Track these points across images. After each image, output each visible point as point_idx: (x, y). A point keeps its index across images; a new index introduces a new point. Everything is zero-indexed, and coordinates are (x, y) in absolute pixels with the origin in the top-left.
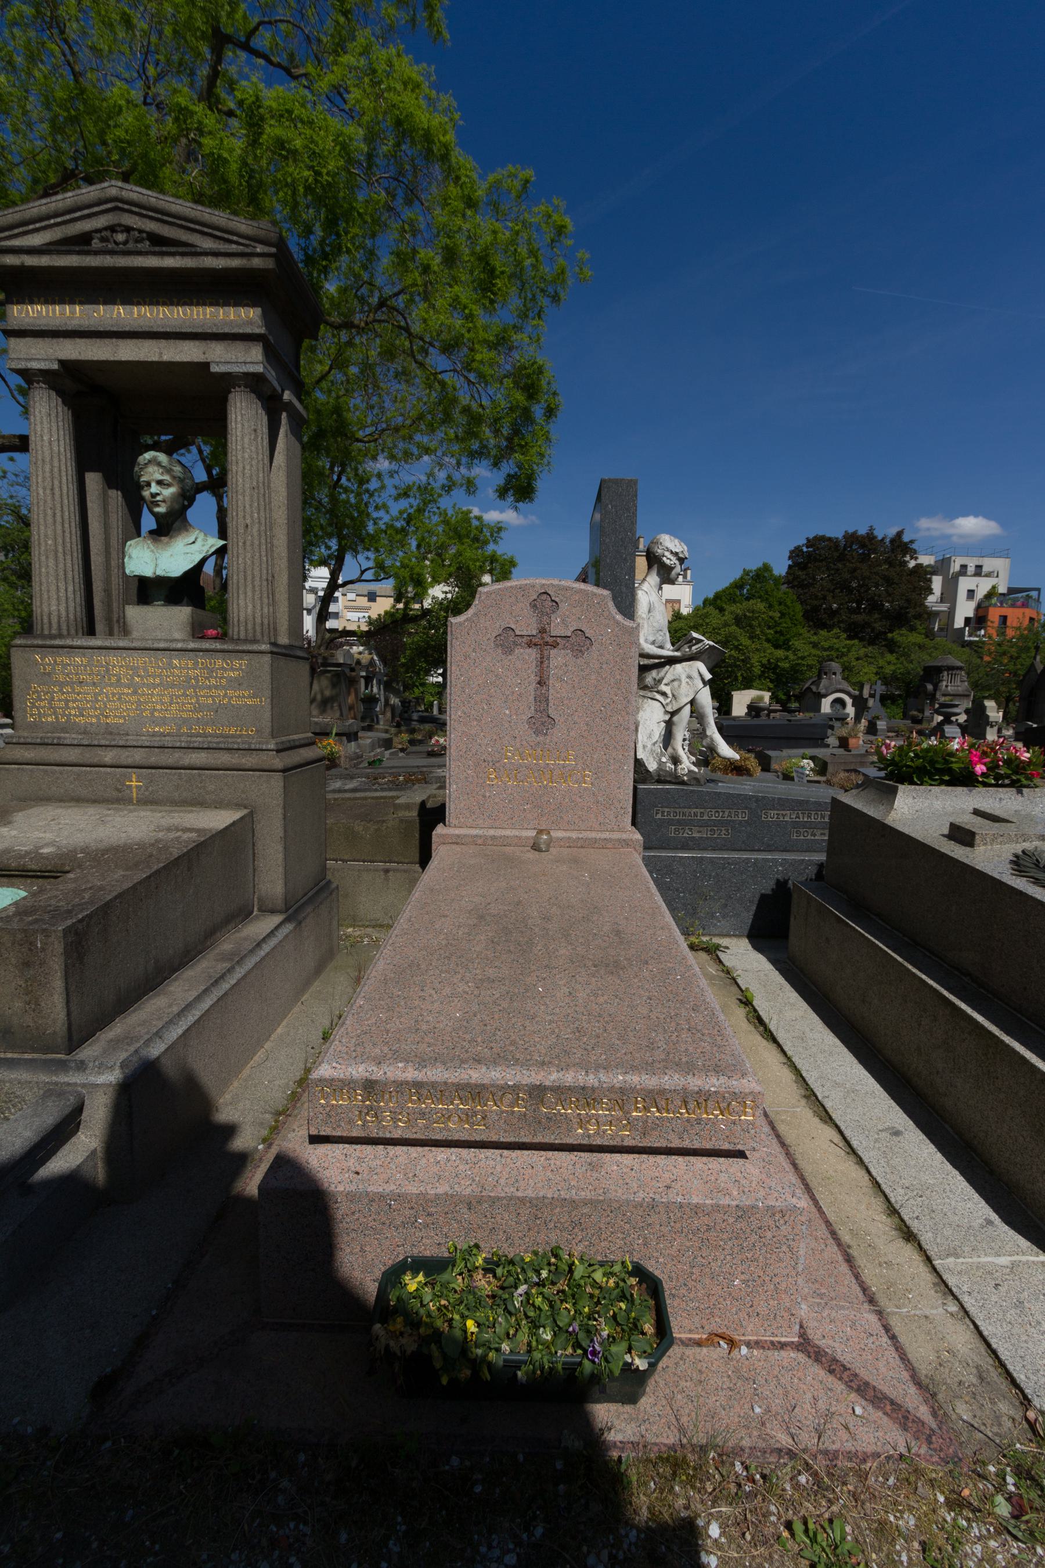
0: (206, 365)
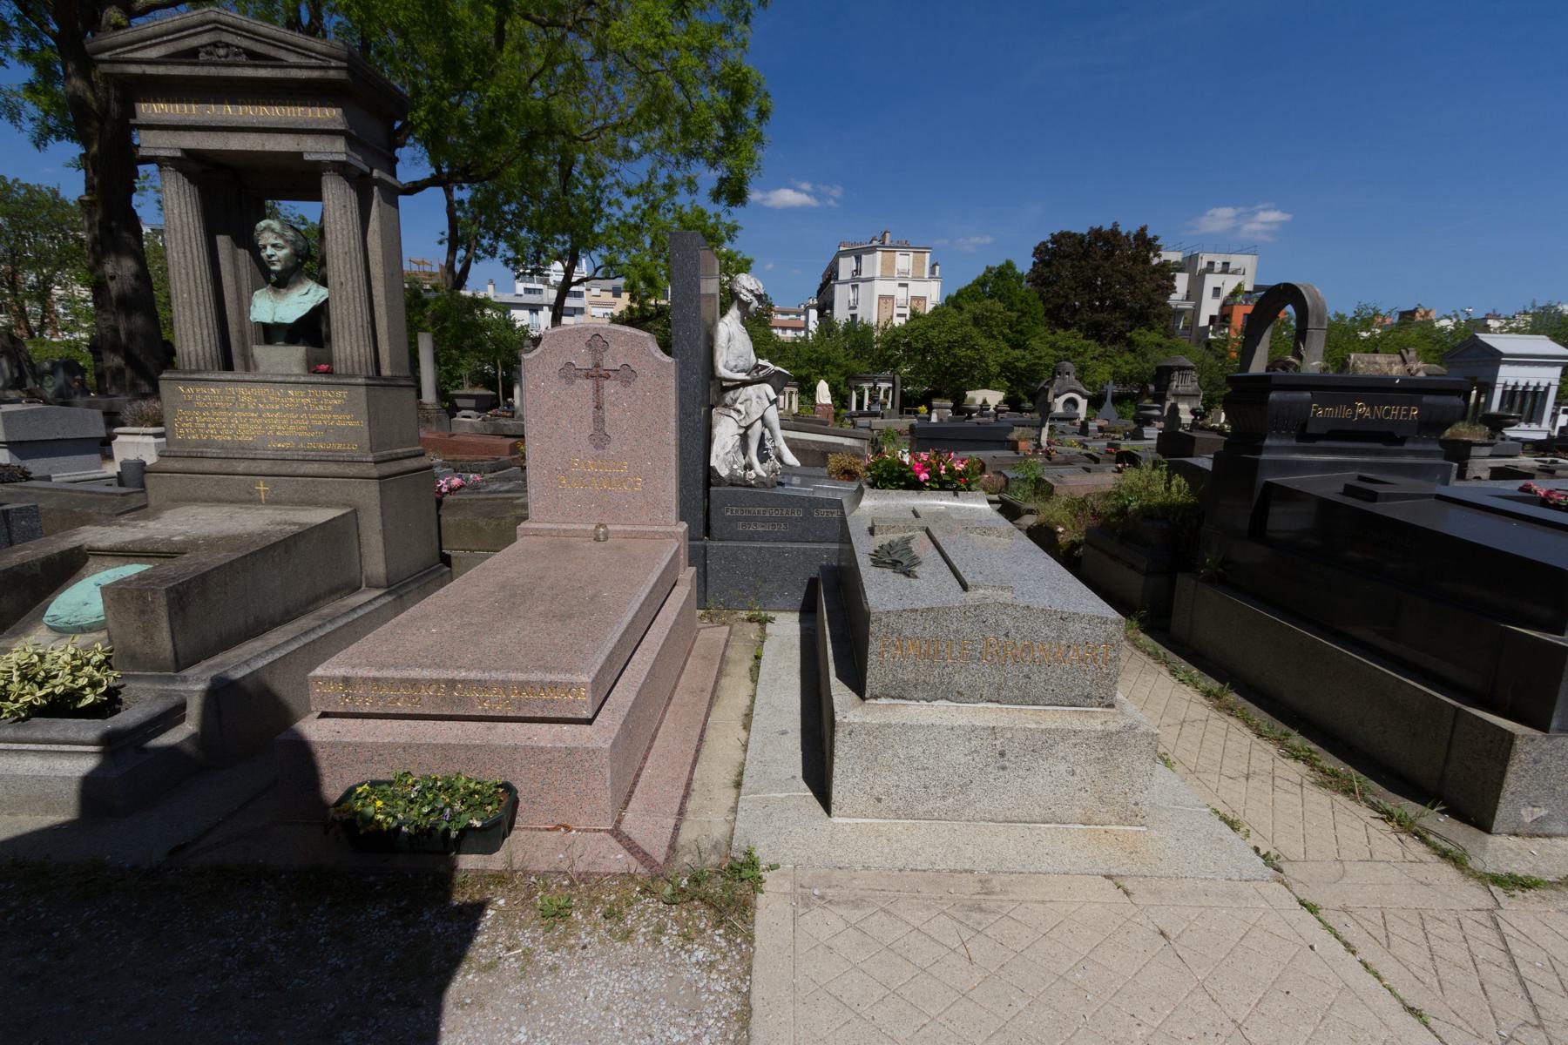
0: (301, 154)
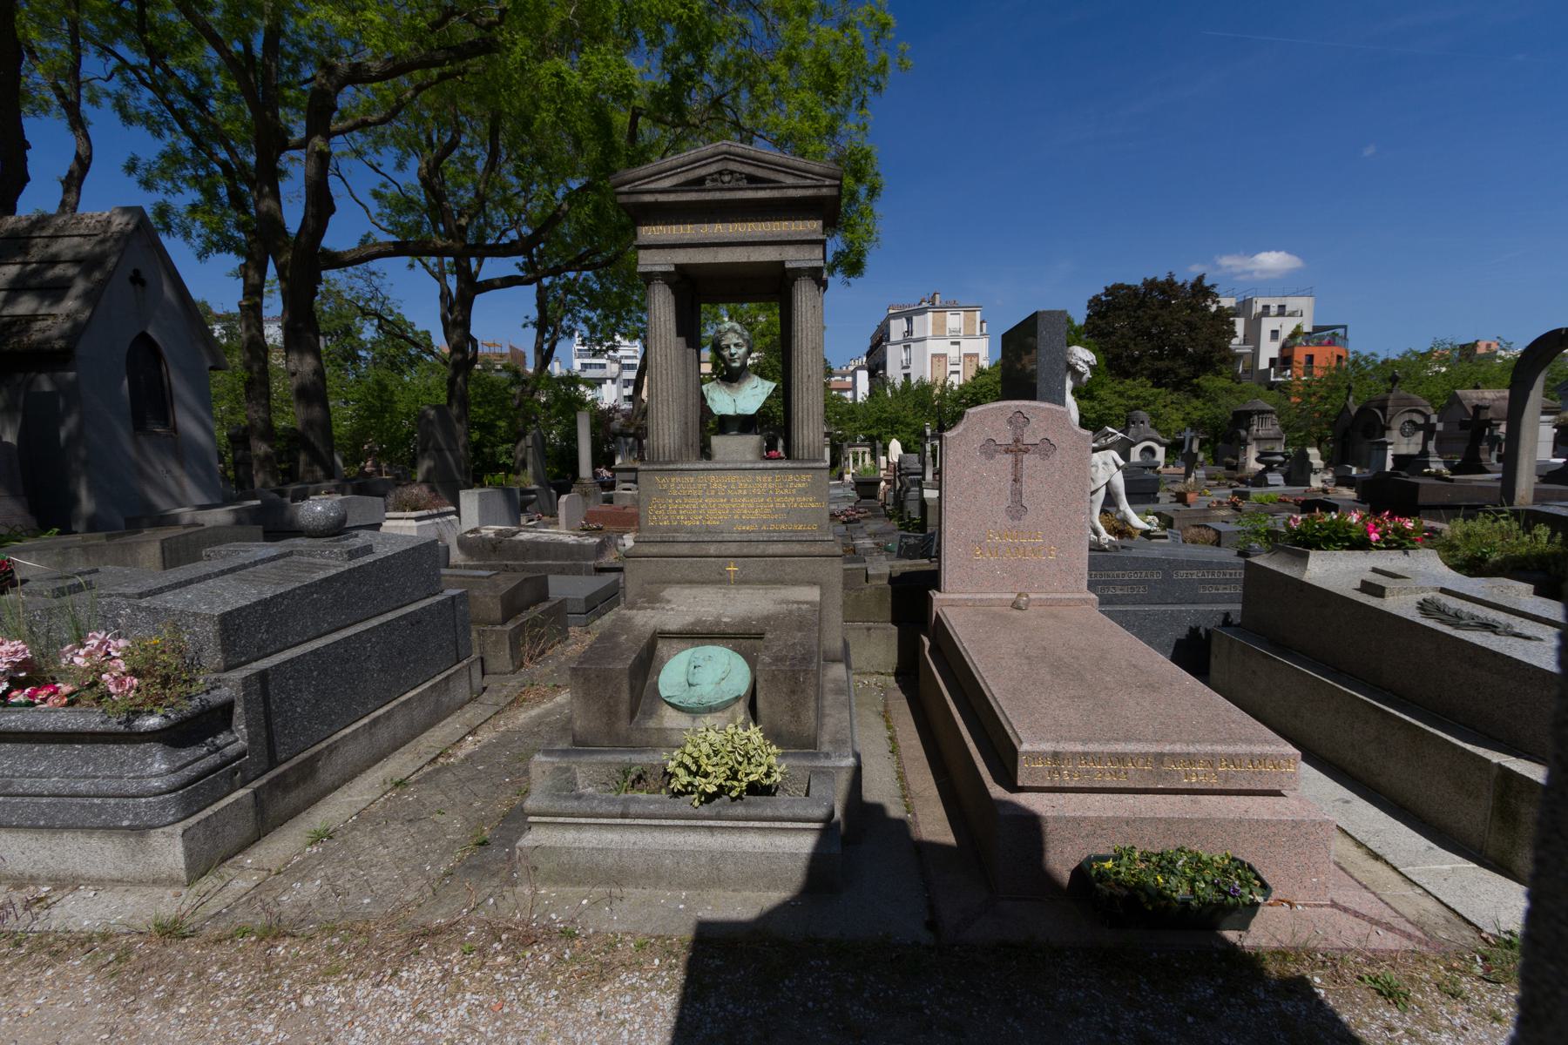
0: (782, 263)
